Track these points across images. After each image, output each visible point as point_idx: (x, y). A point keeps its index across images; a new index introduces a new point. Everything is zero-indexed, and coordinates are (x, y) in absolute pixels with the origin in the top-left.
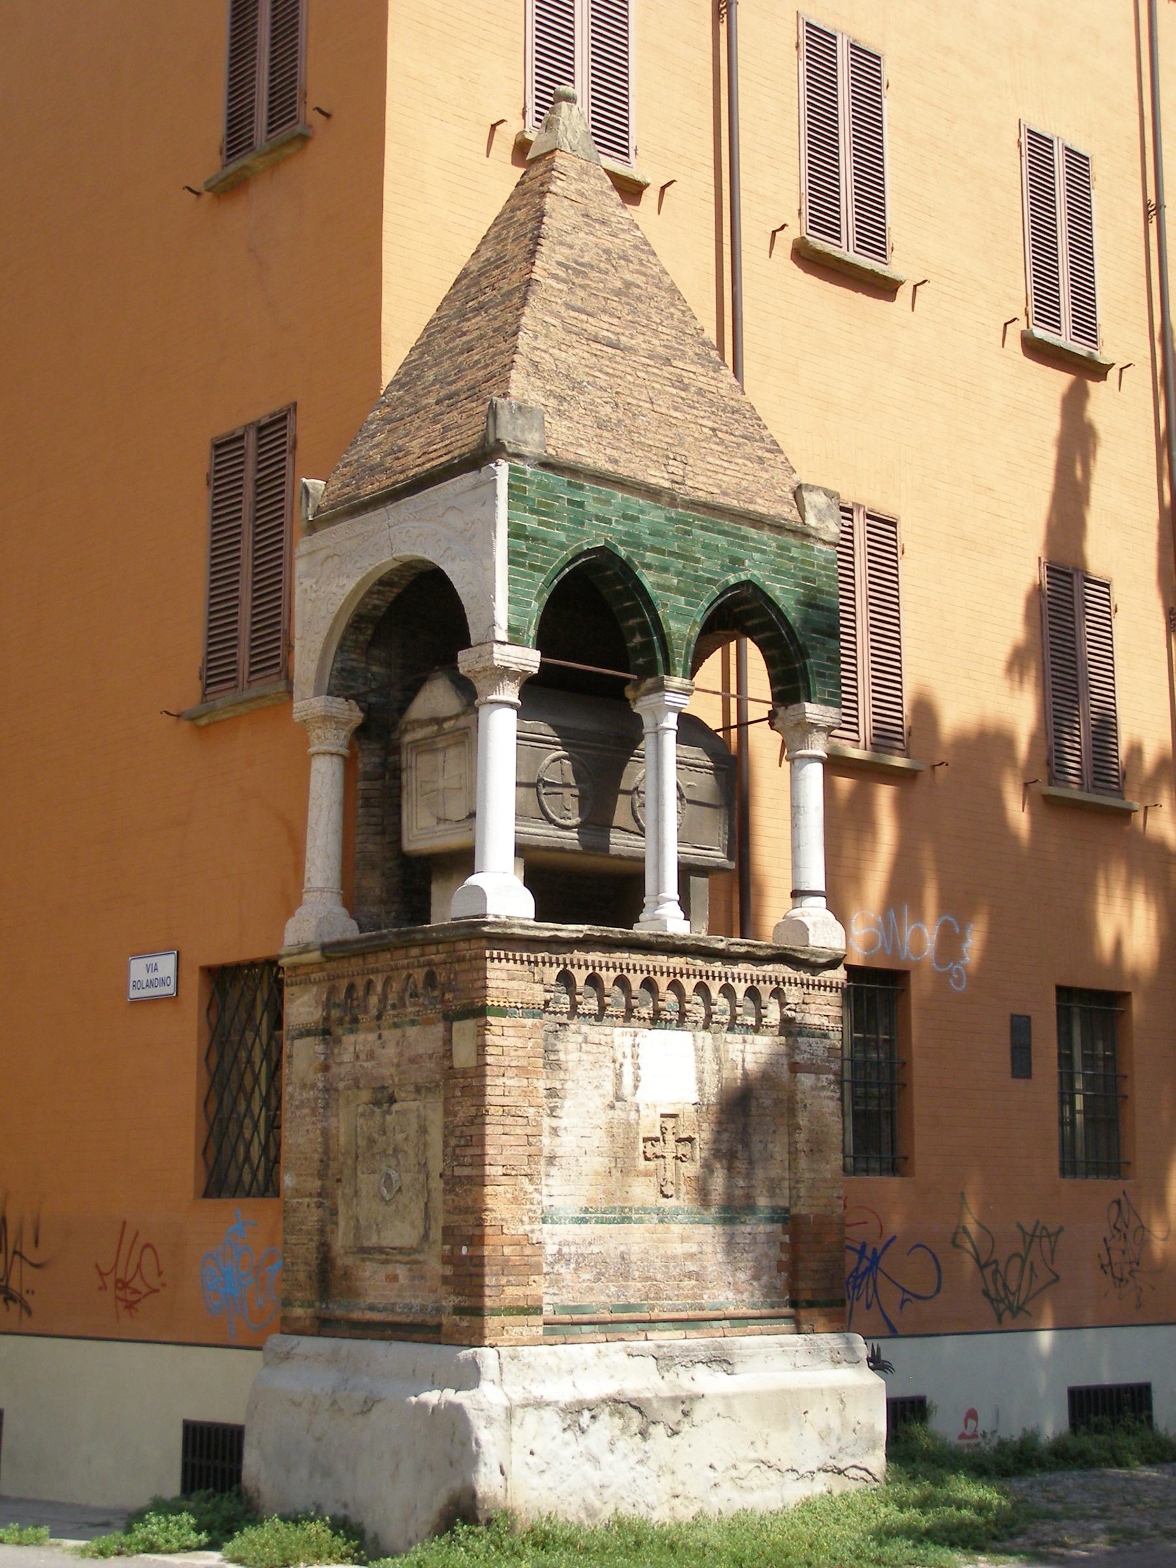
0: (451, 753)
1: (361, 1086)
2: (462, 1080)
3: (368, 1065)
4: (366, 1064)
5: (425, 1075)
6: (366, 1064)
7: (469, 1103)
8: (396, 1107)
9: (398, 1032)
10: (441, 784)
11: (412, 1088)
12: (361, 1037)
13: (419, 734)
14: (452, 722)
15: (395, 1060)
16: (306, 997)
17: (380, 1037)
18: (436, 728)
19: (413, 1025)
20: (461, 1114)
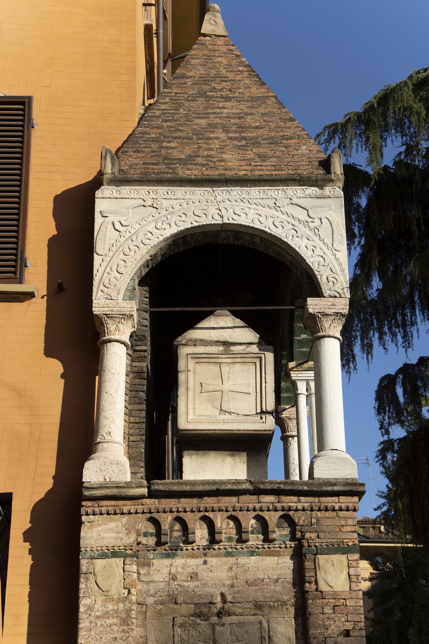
0: (238, 367)
1: (178, 601)
2: (333, 601)
3: (191, 584)
4: (186, 584)
5: (269, 595)
6: (186, 584)
7: (343, 619)
8: (227, 620)
9: (232, 560)
10: (226, 386)
11: (251, 605)
12: (179, 561)
13: (201, 349)
14: (243, 347)
15: (228, 582)
16: (112, 525)
17: (205, 562)
18: (221, 348)
19: (252, 555)
20: (333, 627)
